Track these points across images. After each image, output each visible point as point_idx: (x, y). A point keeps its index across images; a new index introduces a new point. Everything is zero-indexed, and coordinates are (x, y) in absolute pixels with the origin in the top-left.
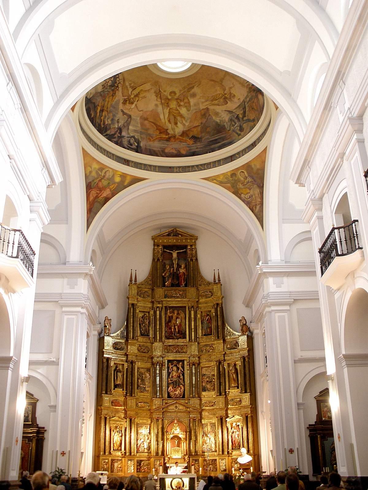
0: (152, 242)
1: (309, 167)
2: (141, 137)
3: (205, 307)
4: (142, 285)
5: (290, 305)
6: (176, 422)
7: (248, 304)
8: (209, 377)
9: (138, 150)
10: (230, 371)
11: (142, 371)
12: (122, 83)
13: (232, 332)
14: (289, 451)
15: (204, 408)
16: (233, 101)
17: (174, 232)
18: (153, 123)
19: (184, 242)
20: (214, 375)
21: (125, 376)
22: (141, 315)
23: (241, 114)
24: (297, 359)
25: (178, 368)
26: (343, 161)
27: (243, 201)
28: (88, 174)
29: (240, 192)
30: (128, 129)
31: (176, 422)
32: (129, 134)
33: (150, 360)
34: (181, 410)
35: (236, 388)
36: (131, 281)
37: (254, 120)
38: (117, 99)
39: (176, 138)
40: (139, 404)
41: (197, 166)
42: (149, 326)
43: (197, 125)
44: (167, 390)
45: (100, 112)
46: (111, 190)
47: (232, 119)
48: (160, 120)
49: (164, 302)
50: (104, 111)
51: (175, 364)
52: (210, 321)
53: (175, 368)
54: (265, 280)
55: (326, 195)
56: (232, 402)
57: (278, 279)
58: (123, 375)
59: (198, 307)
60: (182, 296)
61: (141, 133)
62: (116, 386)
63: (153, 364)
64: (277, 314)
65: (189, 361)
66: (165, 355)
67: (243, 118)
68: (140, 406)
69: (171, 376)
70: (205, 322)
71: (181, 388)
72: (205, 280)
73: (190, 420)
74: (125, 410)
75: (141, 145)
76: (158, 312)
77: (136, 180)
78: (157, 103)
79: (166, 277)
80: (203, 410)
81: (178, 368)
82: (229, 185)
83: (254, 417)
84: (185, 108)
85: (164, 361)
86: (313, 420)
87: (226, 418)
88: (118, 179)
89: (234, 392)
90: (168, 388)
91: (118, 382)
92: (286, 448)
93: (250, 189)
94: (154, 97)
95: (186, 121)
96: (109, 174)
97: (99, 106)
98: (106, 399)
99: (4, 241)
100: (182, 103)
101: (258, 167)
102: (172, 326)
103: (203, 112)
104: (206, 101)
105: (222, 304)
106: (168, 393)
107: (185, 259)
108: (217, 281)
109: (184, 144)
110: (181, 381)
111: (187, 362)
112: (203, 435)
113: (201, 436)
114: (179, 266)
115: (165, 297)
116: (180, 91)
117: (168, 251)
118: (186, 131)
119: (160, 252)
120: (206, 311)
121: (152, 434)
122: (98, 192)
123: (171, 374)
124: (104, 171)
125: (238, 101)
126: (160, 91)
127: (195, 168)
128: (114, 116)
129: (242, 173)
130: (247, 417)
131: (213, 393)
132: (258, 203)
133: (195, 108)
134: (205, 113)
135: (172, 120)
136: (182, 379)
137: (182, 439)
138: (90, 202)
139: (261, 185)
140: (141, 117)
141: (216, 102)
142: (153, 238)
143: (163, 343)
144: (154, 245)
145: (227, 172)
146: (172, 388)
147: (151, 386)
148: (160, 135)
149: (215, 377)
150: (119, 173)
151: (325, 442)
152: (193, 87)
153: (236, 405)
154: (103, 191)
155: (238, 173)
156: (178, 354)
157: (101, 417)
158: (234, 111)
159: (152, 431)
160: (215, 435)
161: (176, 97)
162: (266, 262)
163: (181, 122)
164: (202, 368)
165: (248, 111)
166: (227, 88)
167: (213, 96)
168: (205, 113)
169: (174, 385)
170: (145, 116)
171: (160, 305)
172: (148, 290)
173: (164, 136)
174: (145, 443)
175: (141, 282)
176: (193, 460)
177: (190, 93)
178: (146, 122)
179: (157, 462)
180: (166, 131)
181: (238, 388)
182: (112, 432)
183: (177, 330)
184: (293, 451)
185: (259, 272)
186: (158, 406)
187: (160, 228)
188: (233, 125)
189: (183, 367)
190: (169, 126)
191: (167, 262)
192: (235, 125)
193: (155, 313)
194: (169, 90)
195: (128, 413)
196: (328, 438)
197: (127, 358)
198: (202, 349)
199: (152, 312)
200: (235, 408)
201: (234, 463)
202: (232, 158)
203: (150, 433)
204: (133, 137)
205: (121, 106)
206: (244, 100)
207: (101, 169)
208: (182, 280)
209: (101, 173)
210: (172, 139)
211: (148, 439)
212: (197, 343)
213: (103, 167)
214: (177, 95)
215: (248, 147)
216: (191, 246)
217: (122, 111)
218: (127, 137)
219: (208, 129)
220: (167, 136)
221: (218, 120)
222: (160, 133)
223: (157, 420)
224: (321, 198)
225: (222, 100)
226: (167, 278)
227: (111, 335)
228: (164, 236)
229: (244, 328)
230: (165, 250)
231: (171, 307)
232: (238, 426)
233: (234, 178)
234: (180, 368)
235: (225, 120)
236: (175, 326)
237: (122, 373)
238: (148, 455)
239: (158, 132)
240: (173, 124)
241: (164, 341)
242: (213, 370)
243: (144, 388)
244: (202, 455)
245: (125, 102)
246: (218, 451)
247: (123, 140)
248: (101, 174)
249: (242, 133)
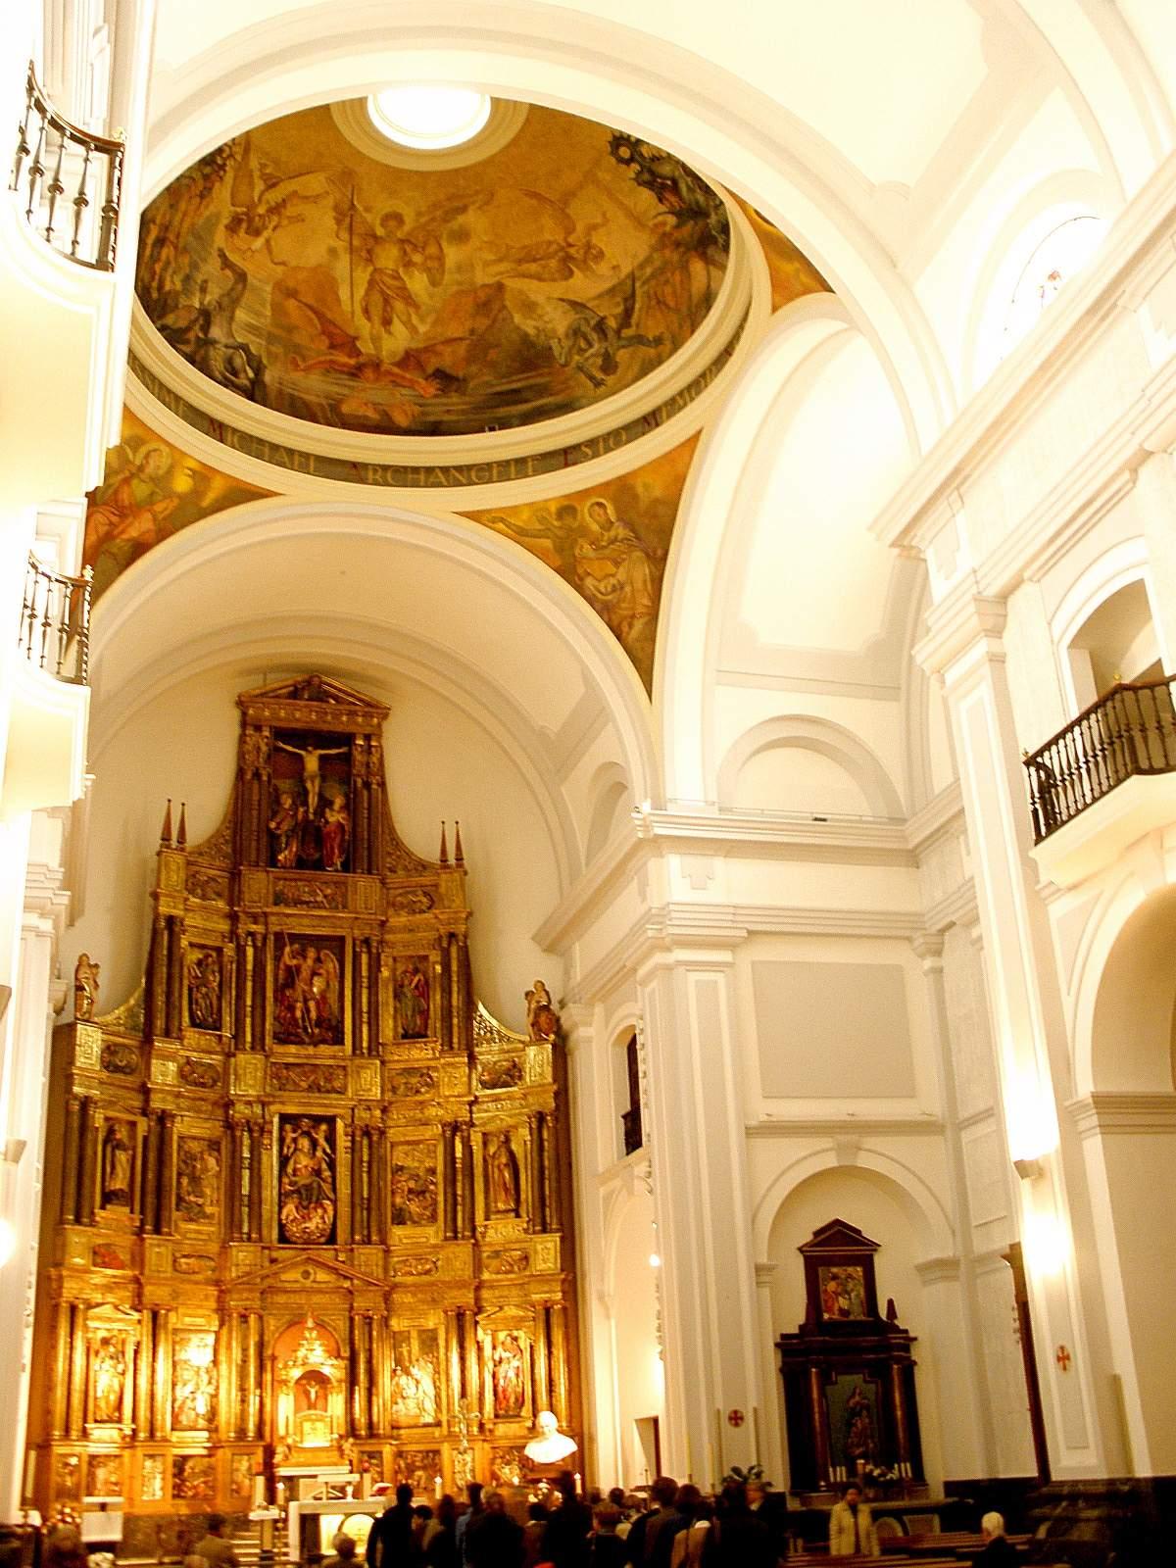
0: (236, 714)
1: (961, 497)
2: (269, 354)
3: (406, 945)
4: (201, 854)
5: (731, 945)
6: (310, 1323)
7: (555, 941)
8: (418, 1176)
9: (254, 392)
10: (490, 1161)
11: (195, 1147)
12: (239, 158)
13: (499, 1032)
14: (730, 1419)
15: (398, 1279)
16: (593, 272)
17: (310, 686)
18: (310, 307)
19: (343, 724)
20: (432, 1171)
21: (139, 1163)
22: (194, 956)
23: (615, 317)
24: (753, 1123)
25: (314, 1144)
26: (1134, 483)
27: (590, 600)
29: (580, 571)
30: (232, 318)
31: (310, 1323)
33: (220, 1112)
34: (323, 1286)
35: (513, 1214)
36: (166, 838)
37: (658, 341)
38: (212, 208)
39: (383, 369)
40: (183, 1260)
41: (445, 470)
42: (220, 998)
43: (456, 335)
44: (276, 1216)
45: (154, 245)
46: (155, 519)
47: (579, 329)
48: (338, 300)
49: (272, 919)
50: (168, 243)
51: (305, 1129)
52: (423, 991)
53: (305, 1143)
54: (653, 864)
55: (1027, 588)
56: (495, 1263)
57: (696, 863)
58: (134, 1157)
59: (381, 942)
60: (332, 903)
61: (271, 338)
62: (108, 1197)
63: (230, 1126)
64: (693, 977)
65: (353, 1121)
66: (274, 1096)
67: (618, 332)
68: (184, 1266)
69: (290, 1170)
70: (408, 991)
71: (325, 1211)
72: (409, 854)
73: (352, 1320)
74: (137, 1281)
75: (267, 377)
76: (250, 951)
77: (243, 494)
79: (280, 835)
80: (395, 1287)
81: (314, 1144)
82: (547, 543)
83: (570, 1312)
84: (425, 275)
85: (267, 1117)
86: (795, 1316)
87: (476, 1314)
88: (182, 484)
89: (502, 1231)
90: (281, 1208)
91: (119, 1183)
92: (721, 1408)
93: (617, 564)
94: (329, 221)
95: (422, 320)
96: (159, 464)
97: (154, 222)
98: (78, 1239)
99: (46, 624)
100: (417, 258)
101: (657, 493)
102: (297, 1001)
103: (482, 296)
104: (500, 260)
105: (466, 937)
106: (282, 1227)
107: (346, 779)
108: (452, 861)
109: (404, 391)
110: (326, 1187)
111: (346, 1126)
112: (395, 1371)
113: (388, 1374)
114: (325, 803)
115: (276, 904)
116: (419, 214)
117: (290, 748)
118: (417, 350)
119: (264, 748)
120: (411, 957)
121: (223, 1367)
122: (115, 519)
123: (292, 1162)
124: (143, 450)
125: (611, 273)
126: (353, 204)
127: (437, 477)
128: (194, 266)
129: (596, 508)
130: (547, 1311)
131: (430, 1231)
132: (640, 610)
133: (457, 277)
134: (490, 300)
135: (376, 313)
136: (330, 1180)
137: (335, 1384)
139: (660, 552)
140: (279, 286)
141: (533, 267)
142: (241, 703)
143: (267, 1057)
144: (244, 724)
145: (546, 501)
146: (297, 1208)
147: (223, 1203)
148: (331, 354)
149: (440, 1178)
150: (192, 464)
151: (829, 1388)
152: (464, 209)
153: (511, 1272)
154: (131, 519)
155: (584, 509)
156: (317, 1095)
157: (56, 1306)
158: (589, 305)
159: (222, 1358)
160: (437, 1372)
161: (399, 235)
162: (658, 804)
163: (404, 318)
164: (392, 1146)
165: (640, 309)
166: (580, 227)
167: (525, 247)
168: (490, 300)
169: (301, 1198)
170: (291, 284)
171: (258, 928)
172: (219, 873)
173: (343, 359)
174: (198, 1395)
175: (199, 846)
176: (363, 1452)
177: (449, 225)
178: (291, 304)
179: (240, 1461)
180: (349, 344)
181: (518, 1216)
182: (92, 1357)
183: (313, 1015)
184: (742, 1418)
185: (640, 835)
186: (248, 1269)
187: (265, 671)
188: (581, 351)
189: (331, 1139)
190: (363, 327)
191: (285, 785)
192: (585, 351)
193: (240, 950)
194: (384, 205)
195: (148, 1290)
196: (839, 1378)
197: (147, 1101)
198: (395, 1084)
199: (229, 950)
200: (508, 1280)
201: (499, 1461)
202: (567, 456)
203: (215, 1362)
204: (245, 348)
205: (220, 239)
206: (633, 273)
208: (332, 848)
210: (369, 373)
211: (210, 1383)
212: (378, 1062)
214: (407, 228)
215: (627, 428)
216: (367, 738)
217: (222, 255)
218: (227, 346)
219: (493, 355)
220: (352, 362)
221: (529, 327)
222: (332, 346)
223: (244, 1318)
224: (1003, 598)
225: (553, 263)
226: (284, 840)
227: (96, 1019)
228: (277, 697)
229: (543, 1019)
230: (281, 745)
231: (294, 938)
232: (515, 1339)
233: (568, 520)
234: (322, 1141)
235: (554, 331)
236: (306, 1001)
237: (130, 1152)
238: (209, 1440)
239: (323, 343)
240: (377, 320)
241: (271, 1049)
242: (431, 1153)
243: (199, 1205)
244: (392, 1437)
246: (445, 1424)
247: (212, 353)
248: (131, 456)
249: (610, 380)
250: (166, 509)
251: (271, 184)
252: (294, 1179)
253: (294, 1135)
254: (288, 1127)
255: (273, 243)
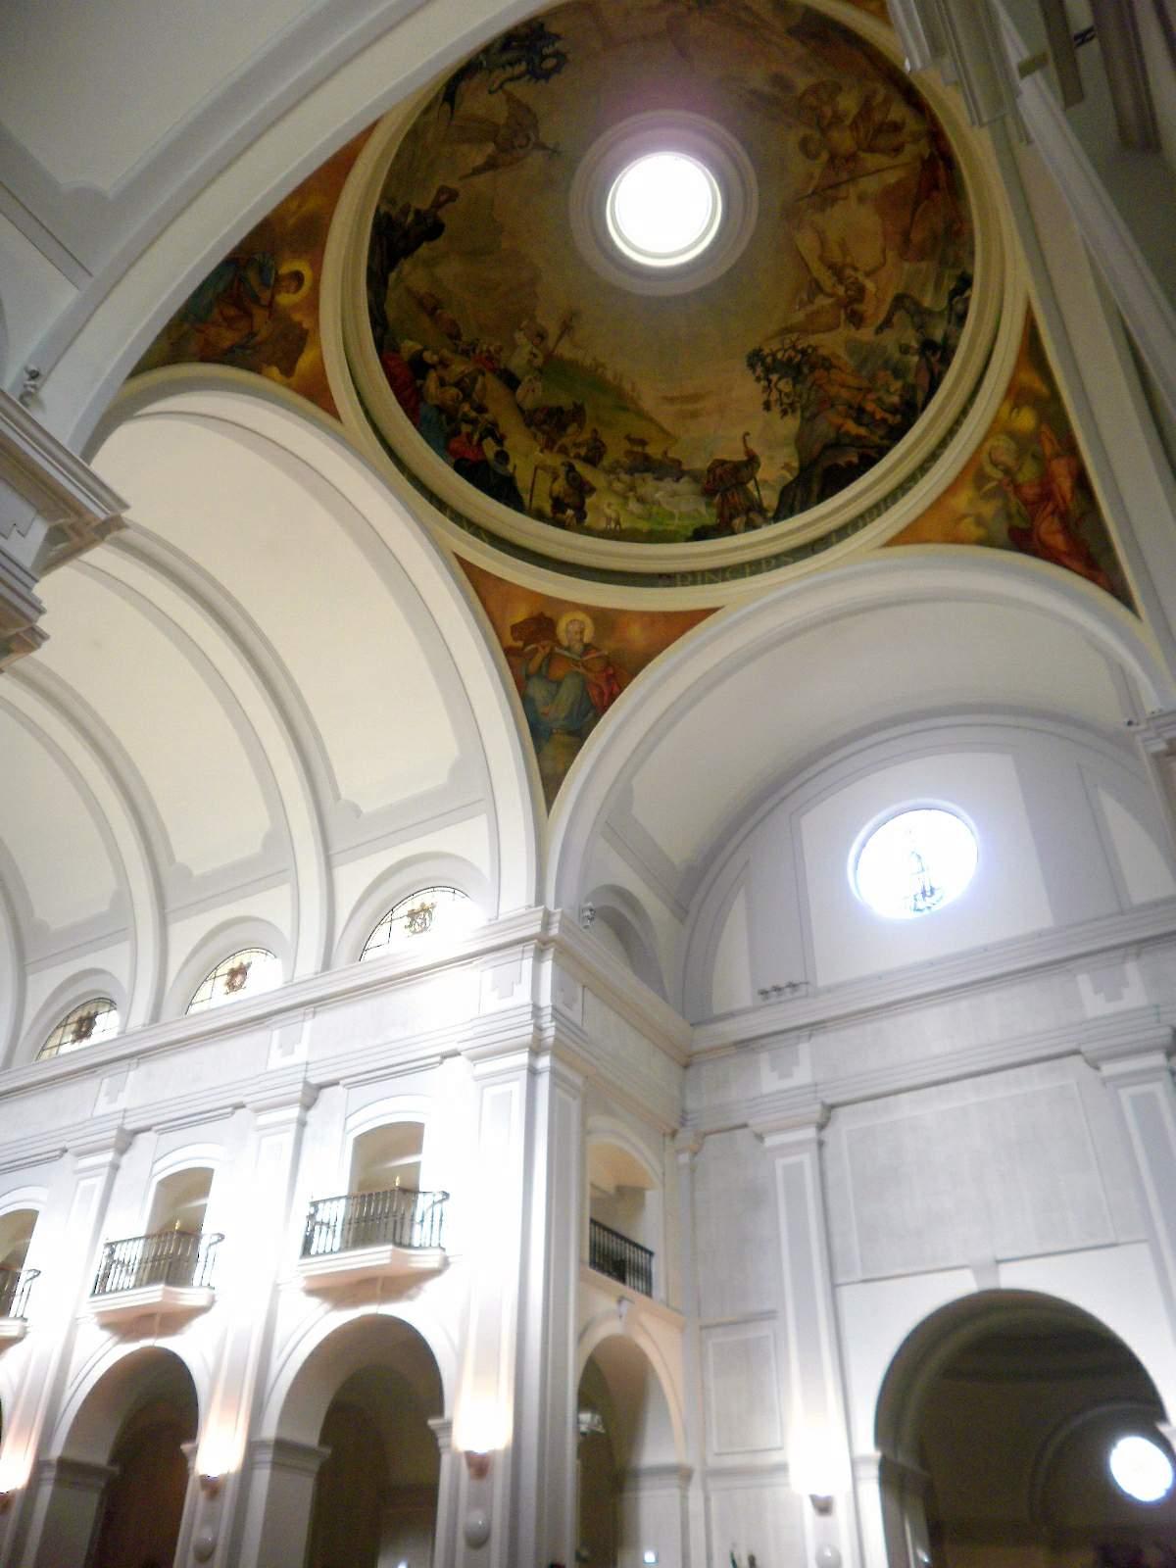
12: (794, 337)
18: (915, 210)
28: (980, 532)
32: (941, 313)
38: (841, 352)
78: (853, 201)
88: (1026, 420)
94: (837, 211)
95: (875, 92)
96: (1003, 447)
100: (828, 111)
122: (1050, 507)
124: (989, 469)
126: (814, 193)
128: (886, 365)
138: (1069, 554)
161: (817, 135)
178: (917, 236)
194: (798, 165)
205: (866, 334)
207: (981, 478)
209: (994, 479)
213: (974, 473)
214: (808, 132)
222: (936, 187)
245: (857, 319)
250: (1050, 440)
251: (817, 288)
255: (868, 269)
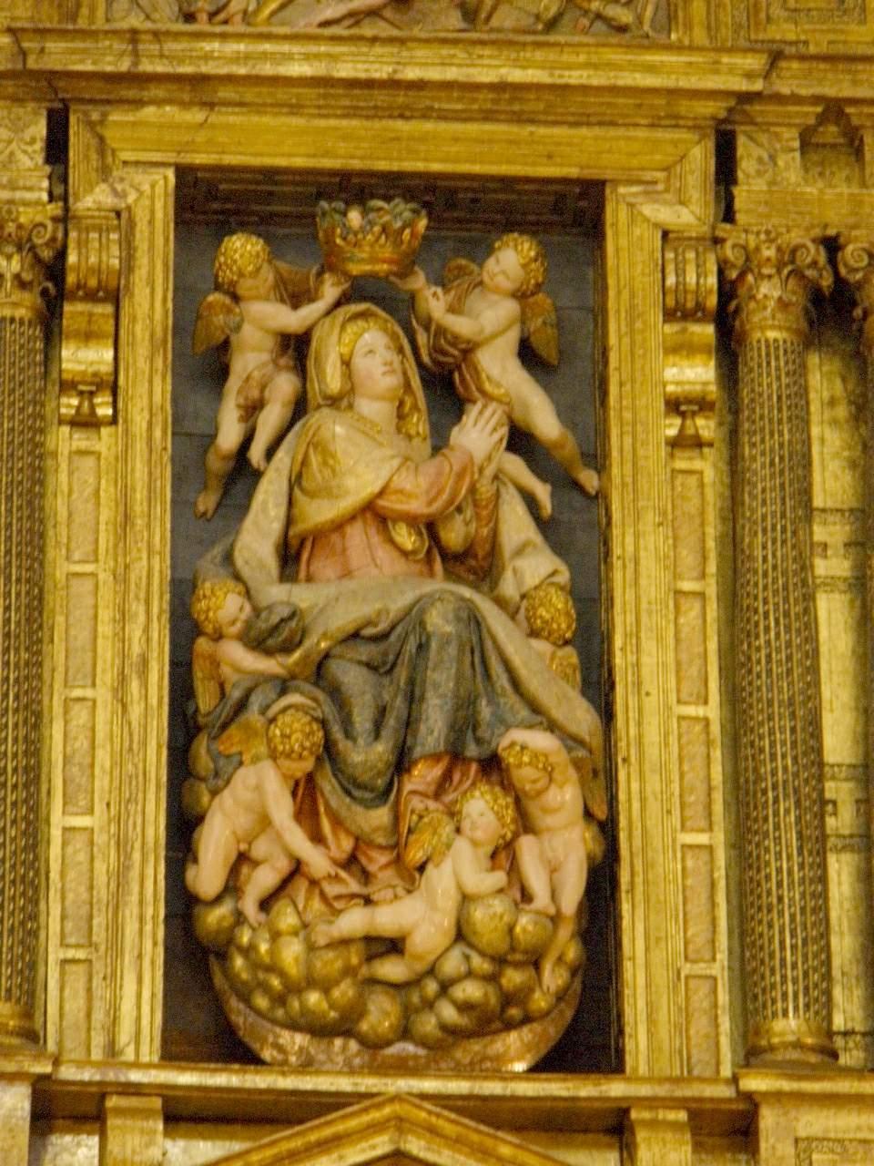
71: (525, 824)
136: (557, 609)
146: (305, 795)
252: (276, 594)
253: (292, 320)
254: (242, 249)
